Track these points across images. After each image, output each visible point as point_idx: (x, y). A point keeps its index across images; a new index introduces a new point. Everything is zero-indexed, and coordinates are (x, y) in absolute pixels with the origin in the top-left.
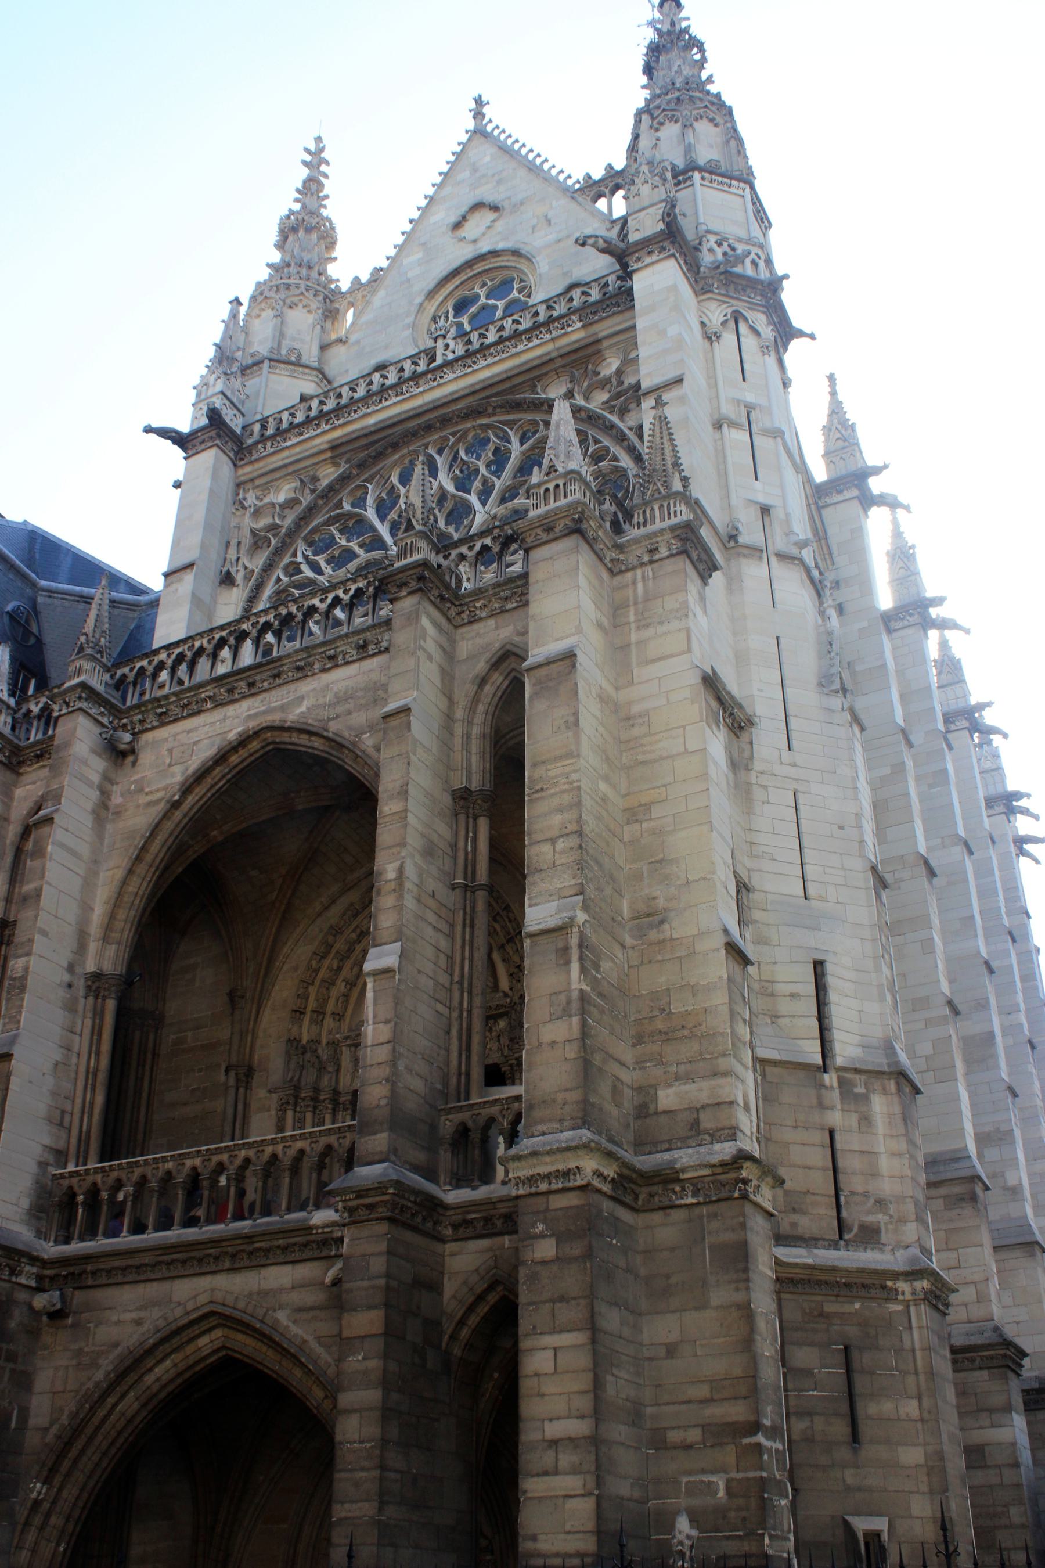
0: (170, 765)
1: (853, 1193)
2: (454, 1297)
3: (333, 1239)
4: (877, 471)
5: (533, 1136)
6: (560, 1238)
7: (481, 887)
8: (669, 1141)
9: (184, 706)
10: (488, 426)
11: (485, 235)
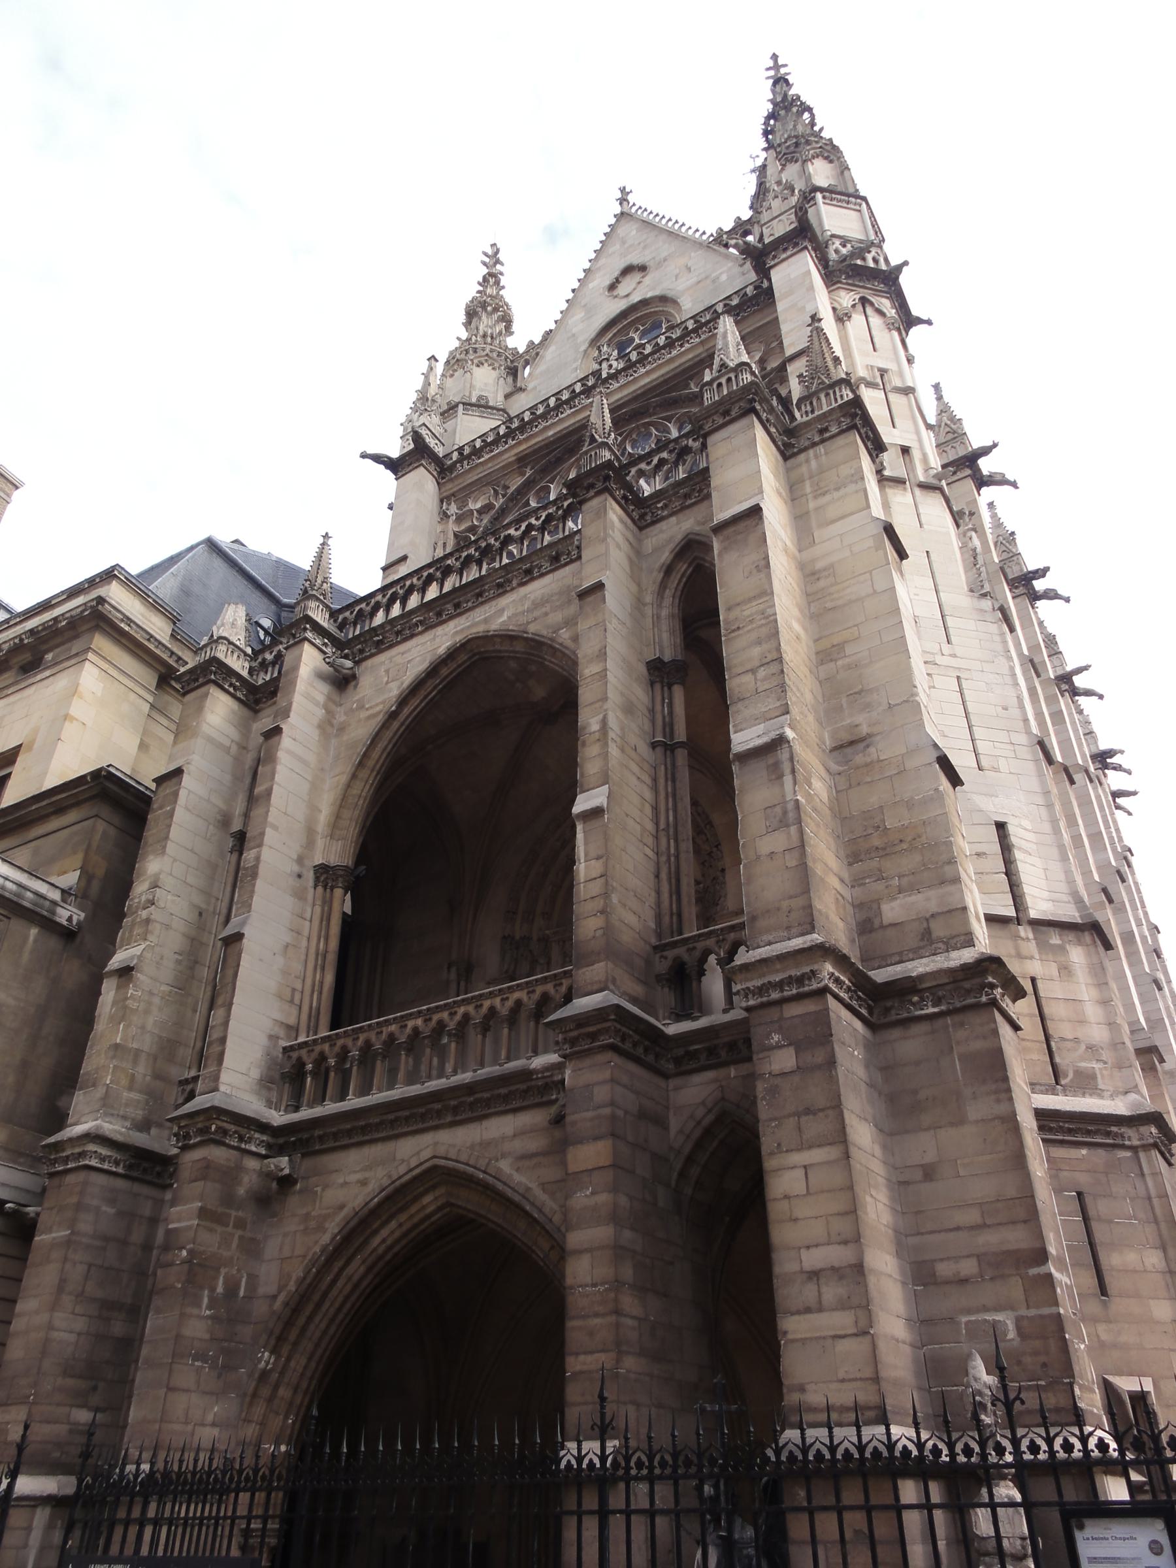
0: (387, 683)
1: (1063, 1039)
2: (681, 1131)
3: (553, 1082)
4: (985, 451)
5: (759, 947)
6: (799, 1047)
7: (681, 745)
8: (900, 953)
9: (398, 633)
10: (650, 424)
11: (636, 290)
